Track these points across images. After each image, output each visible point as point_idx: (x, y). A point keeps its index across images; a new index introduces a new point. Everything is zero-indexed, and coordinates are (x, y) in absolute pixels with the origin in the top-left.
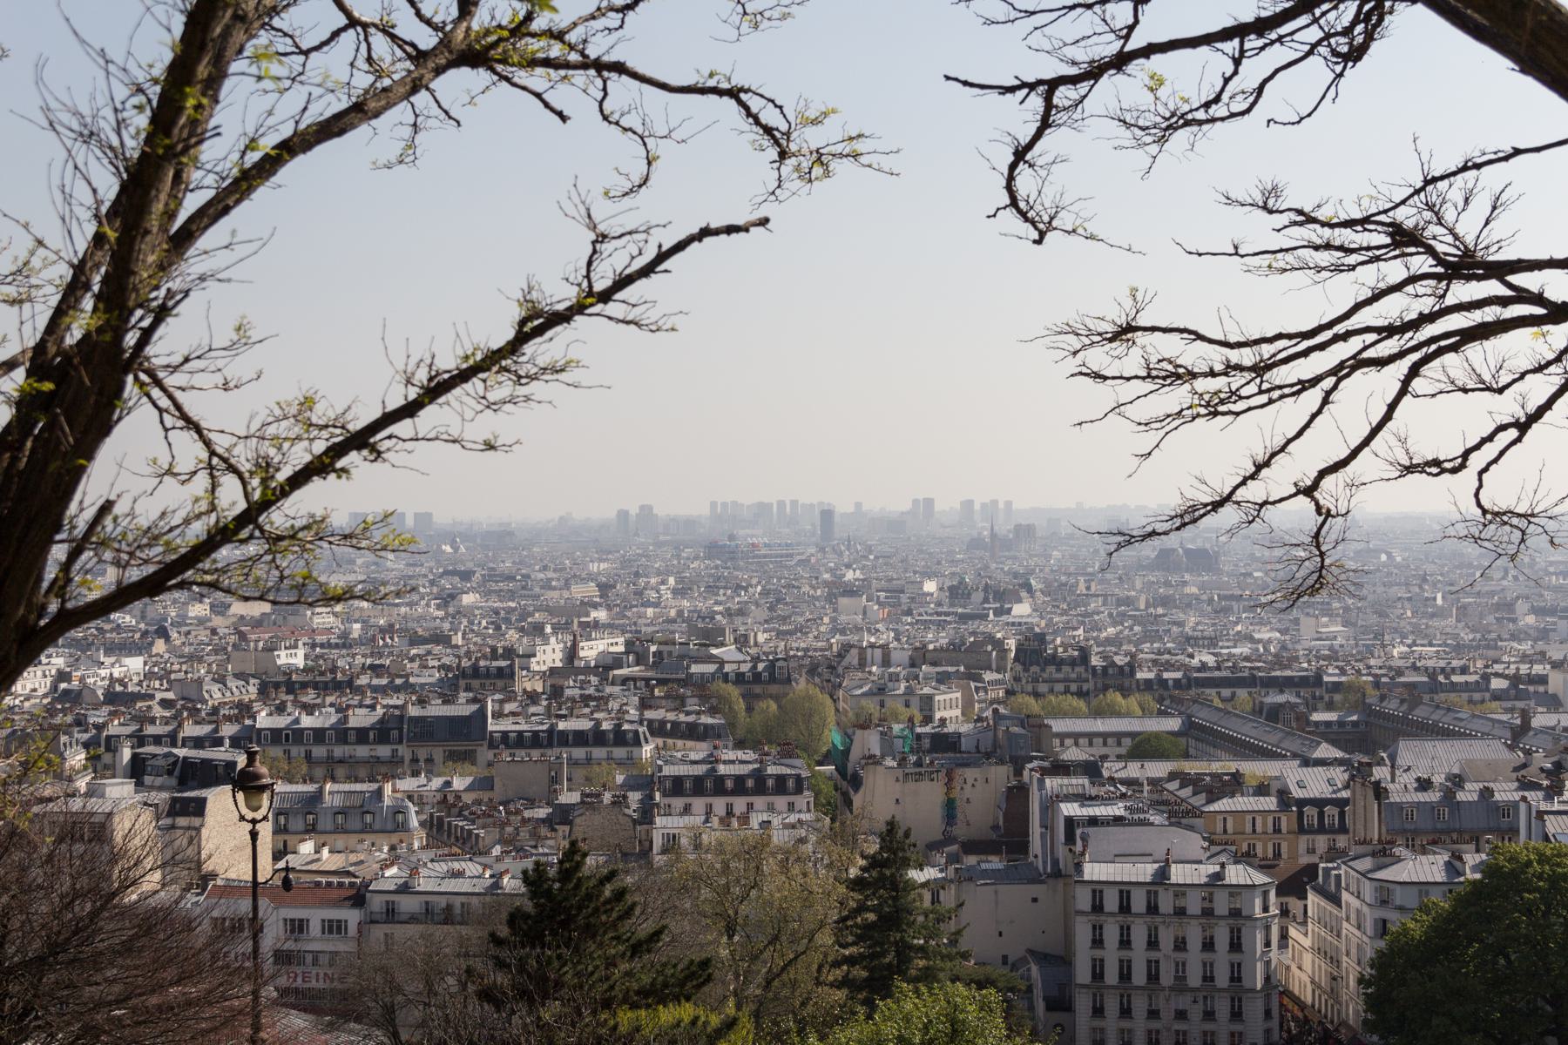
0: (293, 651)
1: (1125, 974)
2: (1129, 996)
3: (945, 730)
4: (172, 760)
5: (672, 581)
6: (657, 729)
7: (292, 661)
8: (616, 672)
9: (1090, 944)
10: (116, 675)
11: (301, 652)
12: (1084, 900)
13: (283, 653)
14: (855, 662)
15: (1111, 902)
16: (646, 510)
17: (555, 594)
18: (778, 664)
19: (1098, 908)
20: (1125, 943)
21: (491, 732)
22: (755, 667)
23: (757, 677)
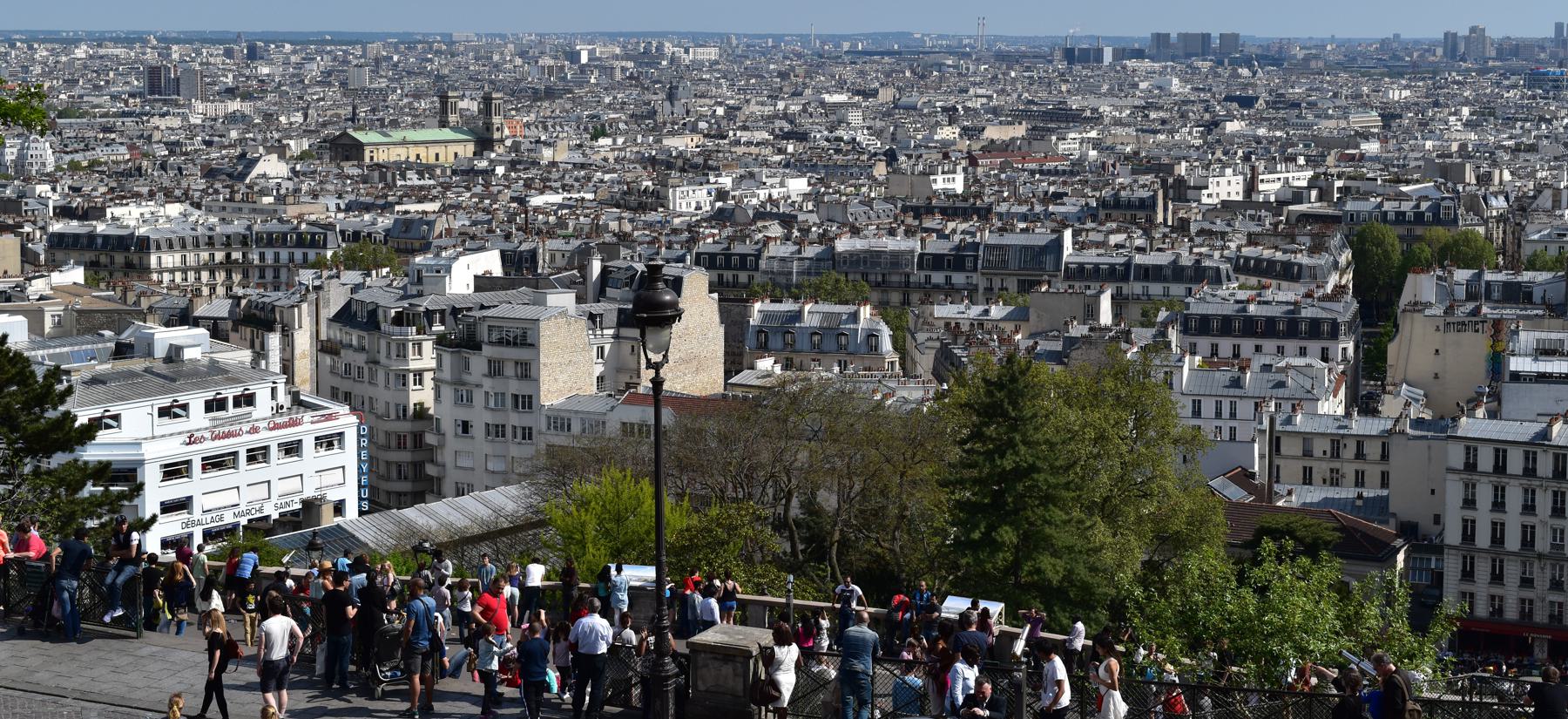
0: (951, 176)
1: (1498, 537)
2: (1502, 561)
3: (1519, 279)
4: (630, 273)
5: (1466, 111)
6: (1242, 267)
7: (949, 186)
8: (1291, 208)
9: (1461, 504)
10: (775, 196)
12: (1456, 456)
14: (1549, 204)
15: (1486, 460)
16: (1397, 36)
17: (1332, 124)
18: (1444, 204)
19: (1471, 467)
20: (1499, 505)
21: (1066, 264)
22: (1418, 206)
23: (1419, 217)
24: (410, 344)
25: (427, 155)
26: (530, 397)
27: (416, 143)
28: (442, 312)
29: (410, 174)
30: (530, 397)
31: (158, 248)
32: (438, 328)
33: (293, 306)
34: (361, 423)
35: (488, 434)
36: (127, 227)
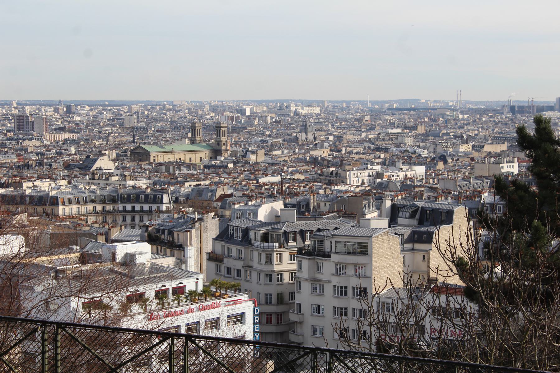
0: (511, 164)
4: (414, 209)
7: (511, 170)
10: (409, 176)
11: (516, 165)
13: (505, 165)
24: (275, 254)
25: (185, 158)
26: (365, 289)
27: (179, 152)
28: (295, 233)
29: (182, 168)
30: (365, 289)
31: (63, 203)
32: (292, 244)
33: (187, 231)
34: (255, 306)
35: (335, 313)
36: (44, 191)
